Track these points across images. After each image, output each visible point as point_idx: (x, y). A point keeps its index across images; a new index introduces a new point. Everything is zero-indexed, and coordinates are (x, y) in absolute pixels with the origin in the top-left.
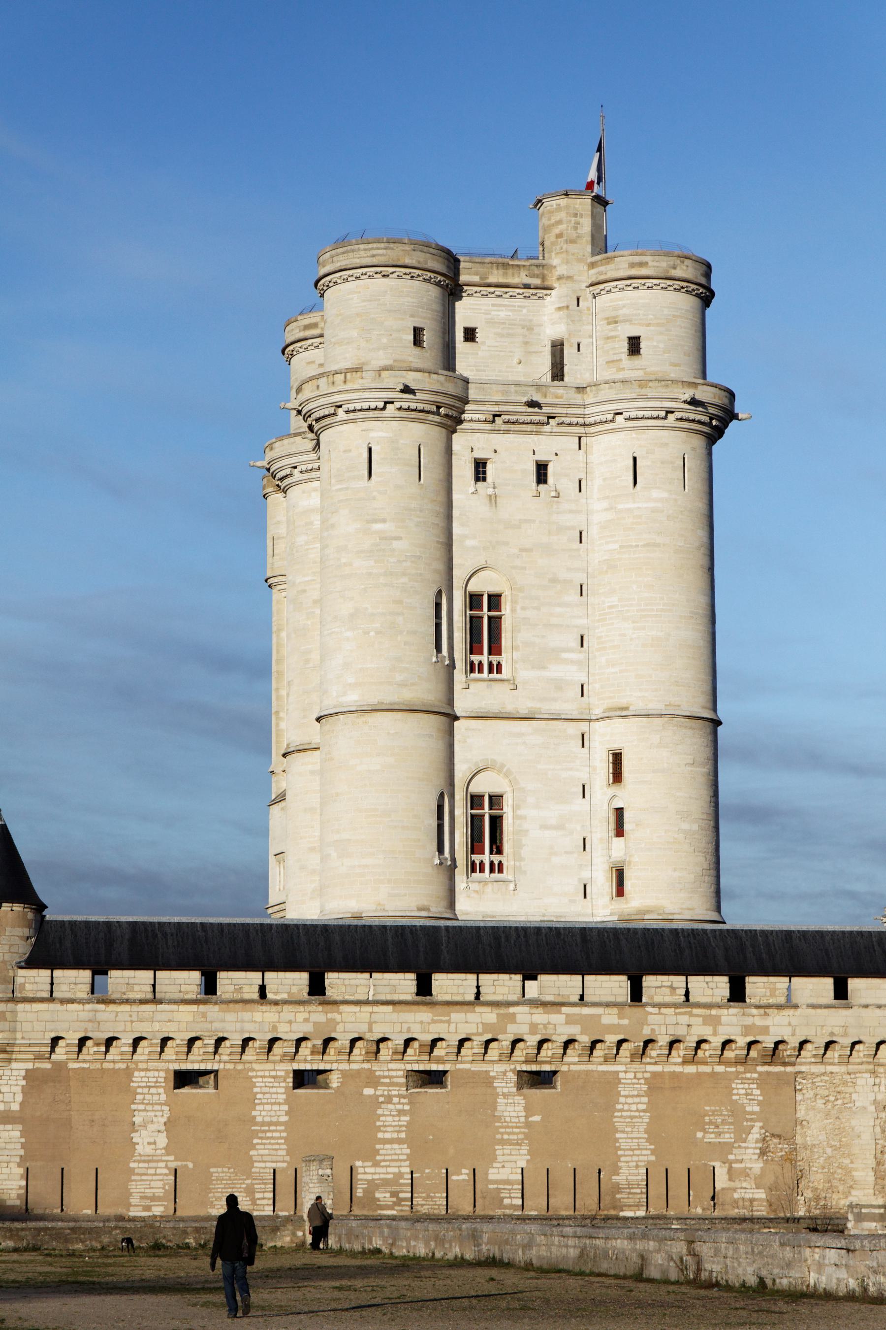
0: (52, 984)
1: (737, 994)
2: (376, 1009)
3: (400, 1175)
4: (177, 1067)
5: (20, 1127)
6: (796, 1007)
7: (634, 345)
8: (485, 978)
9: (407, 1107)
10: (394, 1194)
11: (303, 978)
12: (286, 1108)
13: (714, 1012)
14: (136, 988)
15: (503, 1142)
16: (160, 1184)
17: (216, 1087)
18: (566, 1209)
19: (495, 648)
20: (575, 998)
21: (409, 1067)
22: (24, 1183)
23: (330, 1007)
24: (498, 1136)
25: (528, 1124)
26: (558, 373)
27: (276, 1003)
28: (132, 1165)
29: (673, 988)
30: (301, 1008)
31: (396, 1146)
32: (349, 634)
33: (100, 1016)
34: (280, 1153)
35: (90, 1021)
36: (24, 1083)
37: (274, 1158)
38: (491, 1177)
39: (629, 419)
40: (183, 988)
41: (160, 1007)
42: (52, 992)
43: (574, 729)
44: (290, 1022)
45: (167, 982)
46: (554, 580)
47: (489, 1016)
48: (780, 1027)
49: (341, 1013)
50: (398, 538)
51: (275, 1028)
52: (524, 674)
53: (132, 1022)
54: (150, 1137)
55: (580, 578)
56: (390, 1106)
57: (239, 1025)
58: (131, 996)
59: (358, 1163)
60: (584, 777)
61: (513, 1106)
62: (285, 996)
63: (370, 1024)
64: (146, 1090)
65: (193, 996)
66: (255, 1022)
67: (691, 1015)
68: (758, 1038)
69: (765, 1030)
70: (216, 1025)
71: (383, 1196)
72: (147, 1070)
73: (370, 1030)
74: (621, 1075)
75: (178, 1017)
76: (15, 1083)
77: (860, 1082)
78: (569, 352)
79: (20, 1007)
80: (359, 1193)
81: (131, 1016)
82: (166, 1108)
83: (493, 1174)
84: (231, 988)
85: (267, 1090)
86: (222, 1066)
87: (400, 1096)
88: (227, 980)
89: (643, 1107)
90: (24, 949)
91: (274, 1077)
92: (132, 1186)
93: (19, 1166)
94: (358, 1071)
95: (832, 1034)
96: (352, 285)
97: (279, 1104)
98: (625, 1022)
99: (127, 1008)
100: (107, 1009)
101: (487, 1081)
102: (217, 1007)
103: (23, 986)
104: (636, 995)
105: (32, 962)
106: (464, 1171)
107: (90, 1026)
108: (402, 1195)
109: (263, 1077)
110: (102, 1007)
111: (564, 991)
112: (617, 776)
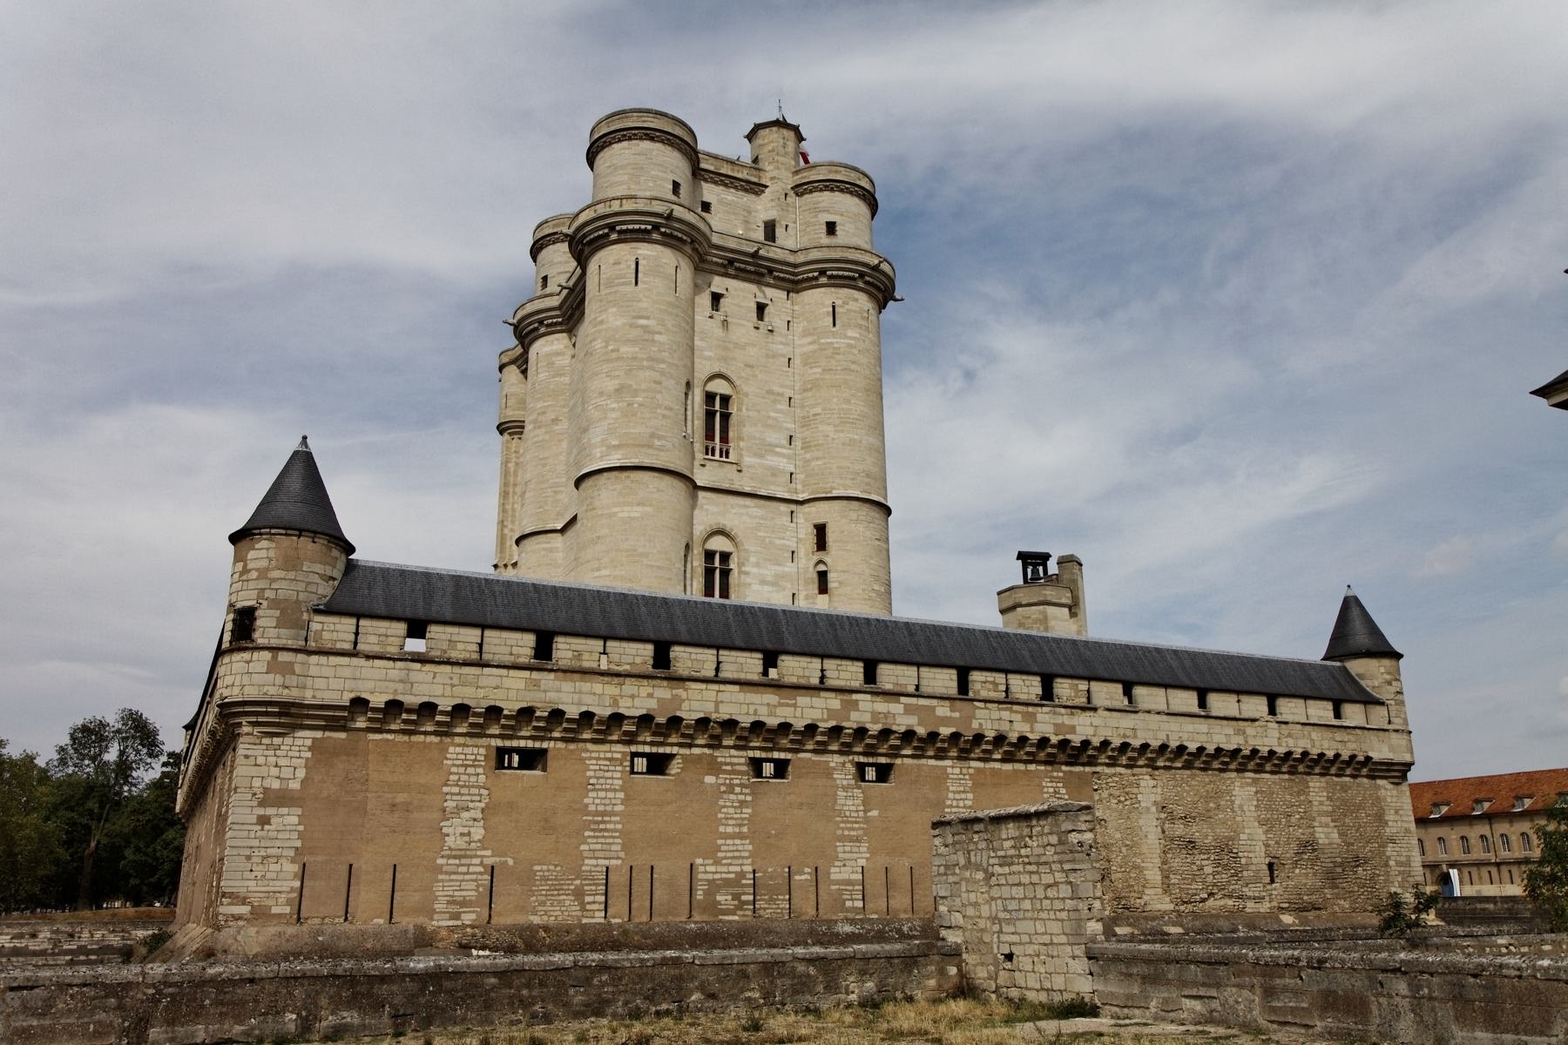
0: (357, 634)
2: (722, 687)
3: (742, 875)
4: (499, 743)
5: (299, 811)
6: (1095, 709)
7: (831, 228)
8: (830, 664)
9: (749, 798)
10: (736, 897)
11: (648, 649)
12: (621, 795)
13: (1030, 709)
14: (460, 646)
15: (843, 839)
16: (473, 885)
17: (544, 770)
18: (905, 911)
19: (725, 439)
20: (911, 689)
21: (751, 754)
22: (297, 884)
23: (675, 683)
24: (839, 832)
25: (866, 817)
28: (440, 861)
29: (996, 684)
30: (645, 682)
31: (738, 842)
33: (414, 676)
34: (614, 848)
36: (309, 755)
37: (608, 854)
38: (833, 877)
39: (830, 277)
40: (515, 650)
41: (486, 670)
42: (356, 643)
43: (784, 508)
44: (633, 697)
45: (496, 641)
46: (770, 392)
47: (834, 702)
48: (1084, 728)
51: (615, 703)
52: (748, 460)
53: (453, 686)
55: (789, 393)
56: (732, 797)
57: (576, 697)
58: (455, 655)
59: (699, 861)
60: (793, 546)
61: (850, 799)
62: (627, 667)
63: (717, 703)
64: (462, 770)
65: (523, 660)
67: (1012, 711)
68: (1068, 737)
69: (1072, 729)
70: (551, 696)
72: (464, 745)
73: (717, 711)
74: (949, 770)
75: (507, 683)
77: (1143, 783)
78: (779, 232)
79: (314, 659)
80: (699, 895)
82: (484, 792)
83: (837, 873)
84: (570, 654)
85: (601, 774)
86: (552, 744)
87: (742, 786)
88: (564, 649)
89: (969, 803)
90: (326, 590)
91: (610, 759)
92: (438, 887)
93: (293, 862)
94: (700, 756)
95: (1125, 736)
96: (625, 144)
97: (615, 790)
98: (957, 715)
99: (448, 668)
101: (828, 773)
102: (552, 675)
103: (319, 633)
104: (963, 686)
105: (329, 610)
106: (807, 870)
107: (400, 687)
108: (744, 898)
109: (598, 759)
110: (418, 666)
111: (902, 681)
112: (821, 545)
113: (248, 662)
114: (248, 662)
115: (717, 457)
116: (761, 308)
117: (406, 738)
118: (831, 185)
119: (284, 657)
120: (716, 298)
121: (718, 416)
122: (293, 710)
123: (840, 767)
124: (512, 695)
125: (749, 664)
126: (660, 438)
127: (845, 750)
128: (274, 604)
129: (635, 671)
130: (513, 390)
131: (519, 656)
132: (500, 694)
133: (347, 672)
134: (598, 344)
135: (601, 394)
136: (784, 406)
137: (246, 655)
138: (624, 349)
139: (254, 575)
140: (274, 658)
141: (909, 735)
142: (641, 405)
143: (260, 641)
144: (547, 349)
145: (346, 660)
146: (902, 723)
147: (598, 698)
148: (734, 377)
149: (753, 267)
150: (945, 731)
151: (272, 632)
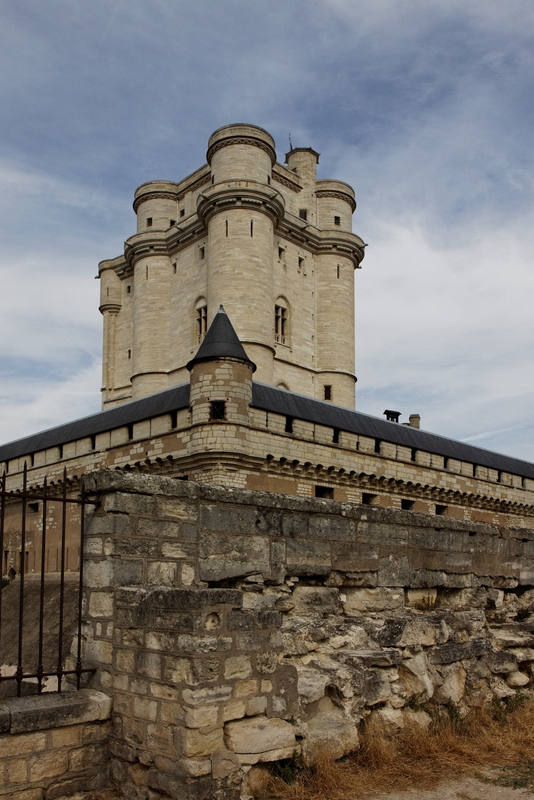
27: (363, 454)
30: (372, 458)
32: (240, 306)
35: (285, 448)
36: (246, 483)
42: (267, 426)
44: (368, 465)
49: (386, 464)
50: (263, 267)
53: (305, 453)
66: (355, 462)
70: (340, 461)
76: (241, 482)
81: (304, 449)
84: (346, 441)
100: (294, 442)
107: (285, 450)
113: (225, 431)
114: (225, 431)
115: (280, 342)
117: (280, 478)
119: (242, 430)
122: (244, 459)
124: (326, 459)
125: (405, 454)
126: (265, 328)
128: (235, 400)
129: (369, 453)
130: (112, 285)
131: (328, 440)
132: (322, 459)
133: (264, 441)
134: (227, 268)
135: (231, 298)
137: (223, 427)
138: (245, 274)
139: (222, 383)
140: (238, 430)
142: (255, 308)
143: (230, 420)
144: (155, 264)
145: (263, 434)
148: (289, 299)
151: (236, 416)
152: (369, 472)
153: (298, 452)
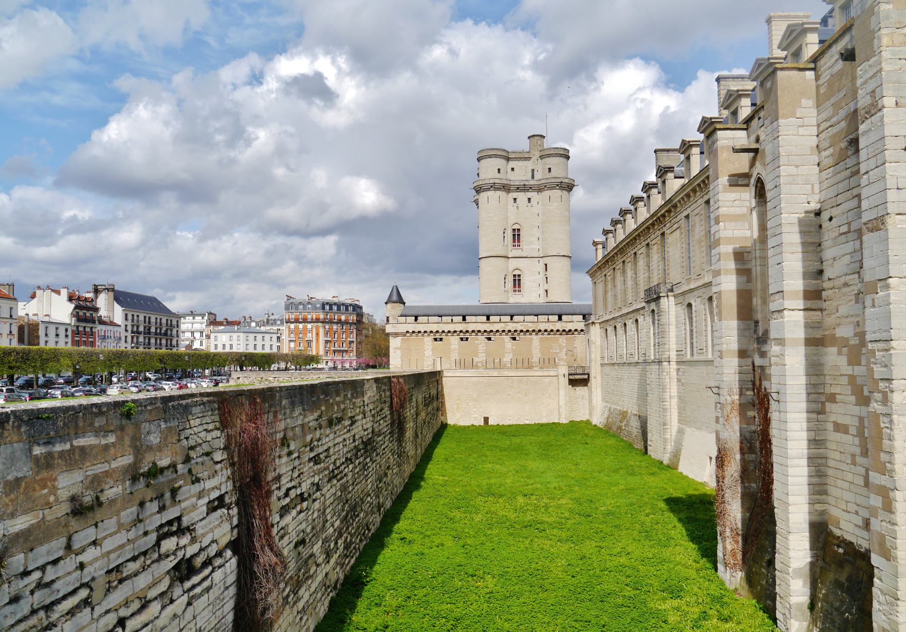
1: (560, 319)
7: (550, 169)
26: (533, 177)
43: (537, 259)
47: (503, 325)
54: (428, 353)
71: (480, 365)
78: (535, 172)
101: (503, 339)
116: (529, 199)
118: (549, 156)
120: (515, 199)
121: (517, 236)
123: (507, 338)
127: (507, 334)
136: (536, 229)
141: (522, 331)
146: (519, 329)
147: (452, 328)
149: (524, 188)
150: (531, 330)
152: (458, 329)
153: (422, 328)
